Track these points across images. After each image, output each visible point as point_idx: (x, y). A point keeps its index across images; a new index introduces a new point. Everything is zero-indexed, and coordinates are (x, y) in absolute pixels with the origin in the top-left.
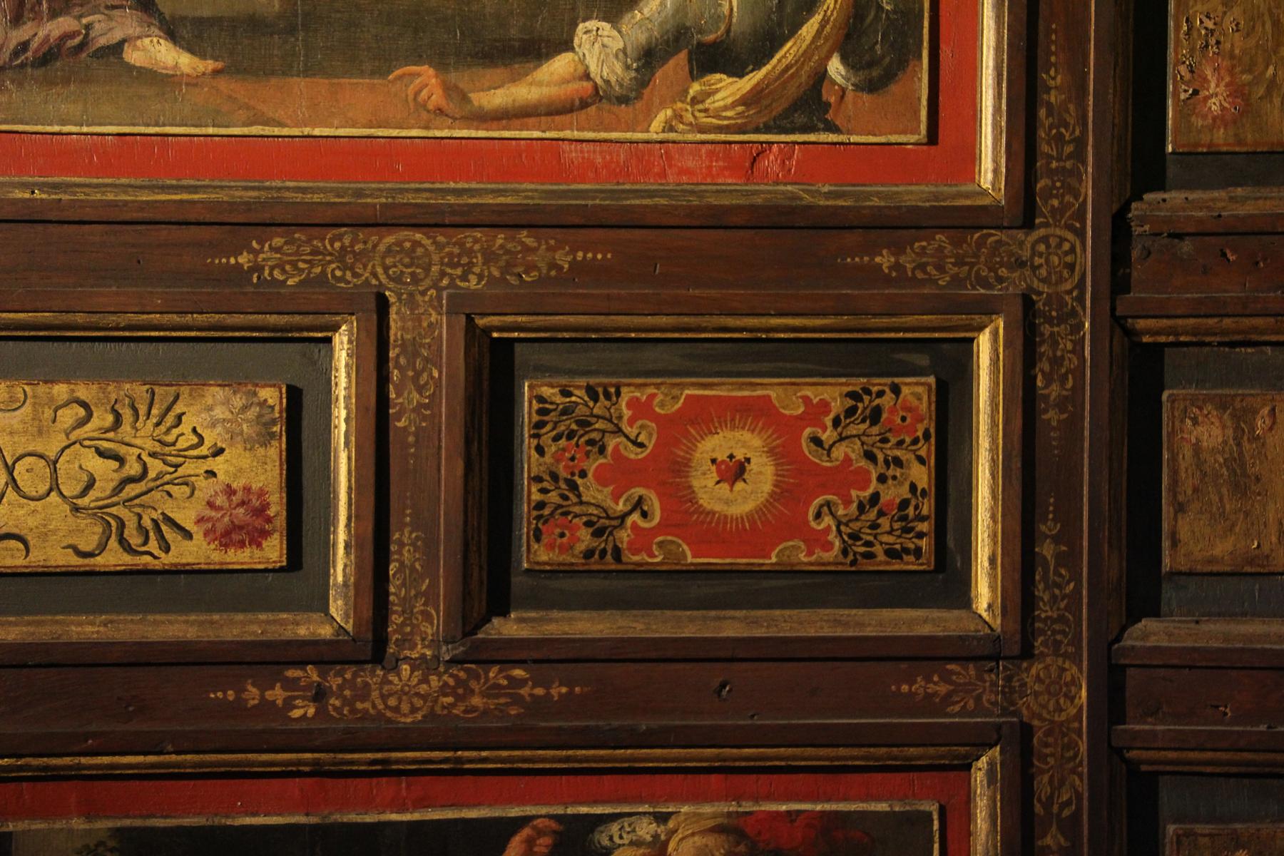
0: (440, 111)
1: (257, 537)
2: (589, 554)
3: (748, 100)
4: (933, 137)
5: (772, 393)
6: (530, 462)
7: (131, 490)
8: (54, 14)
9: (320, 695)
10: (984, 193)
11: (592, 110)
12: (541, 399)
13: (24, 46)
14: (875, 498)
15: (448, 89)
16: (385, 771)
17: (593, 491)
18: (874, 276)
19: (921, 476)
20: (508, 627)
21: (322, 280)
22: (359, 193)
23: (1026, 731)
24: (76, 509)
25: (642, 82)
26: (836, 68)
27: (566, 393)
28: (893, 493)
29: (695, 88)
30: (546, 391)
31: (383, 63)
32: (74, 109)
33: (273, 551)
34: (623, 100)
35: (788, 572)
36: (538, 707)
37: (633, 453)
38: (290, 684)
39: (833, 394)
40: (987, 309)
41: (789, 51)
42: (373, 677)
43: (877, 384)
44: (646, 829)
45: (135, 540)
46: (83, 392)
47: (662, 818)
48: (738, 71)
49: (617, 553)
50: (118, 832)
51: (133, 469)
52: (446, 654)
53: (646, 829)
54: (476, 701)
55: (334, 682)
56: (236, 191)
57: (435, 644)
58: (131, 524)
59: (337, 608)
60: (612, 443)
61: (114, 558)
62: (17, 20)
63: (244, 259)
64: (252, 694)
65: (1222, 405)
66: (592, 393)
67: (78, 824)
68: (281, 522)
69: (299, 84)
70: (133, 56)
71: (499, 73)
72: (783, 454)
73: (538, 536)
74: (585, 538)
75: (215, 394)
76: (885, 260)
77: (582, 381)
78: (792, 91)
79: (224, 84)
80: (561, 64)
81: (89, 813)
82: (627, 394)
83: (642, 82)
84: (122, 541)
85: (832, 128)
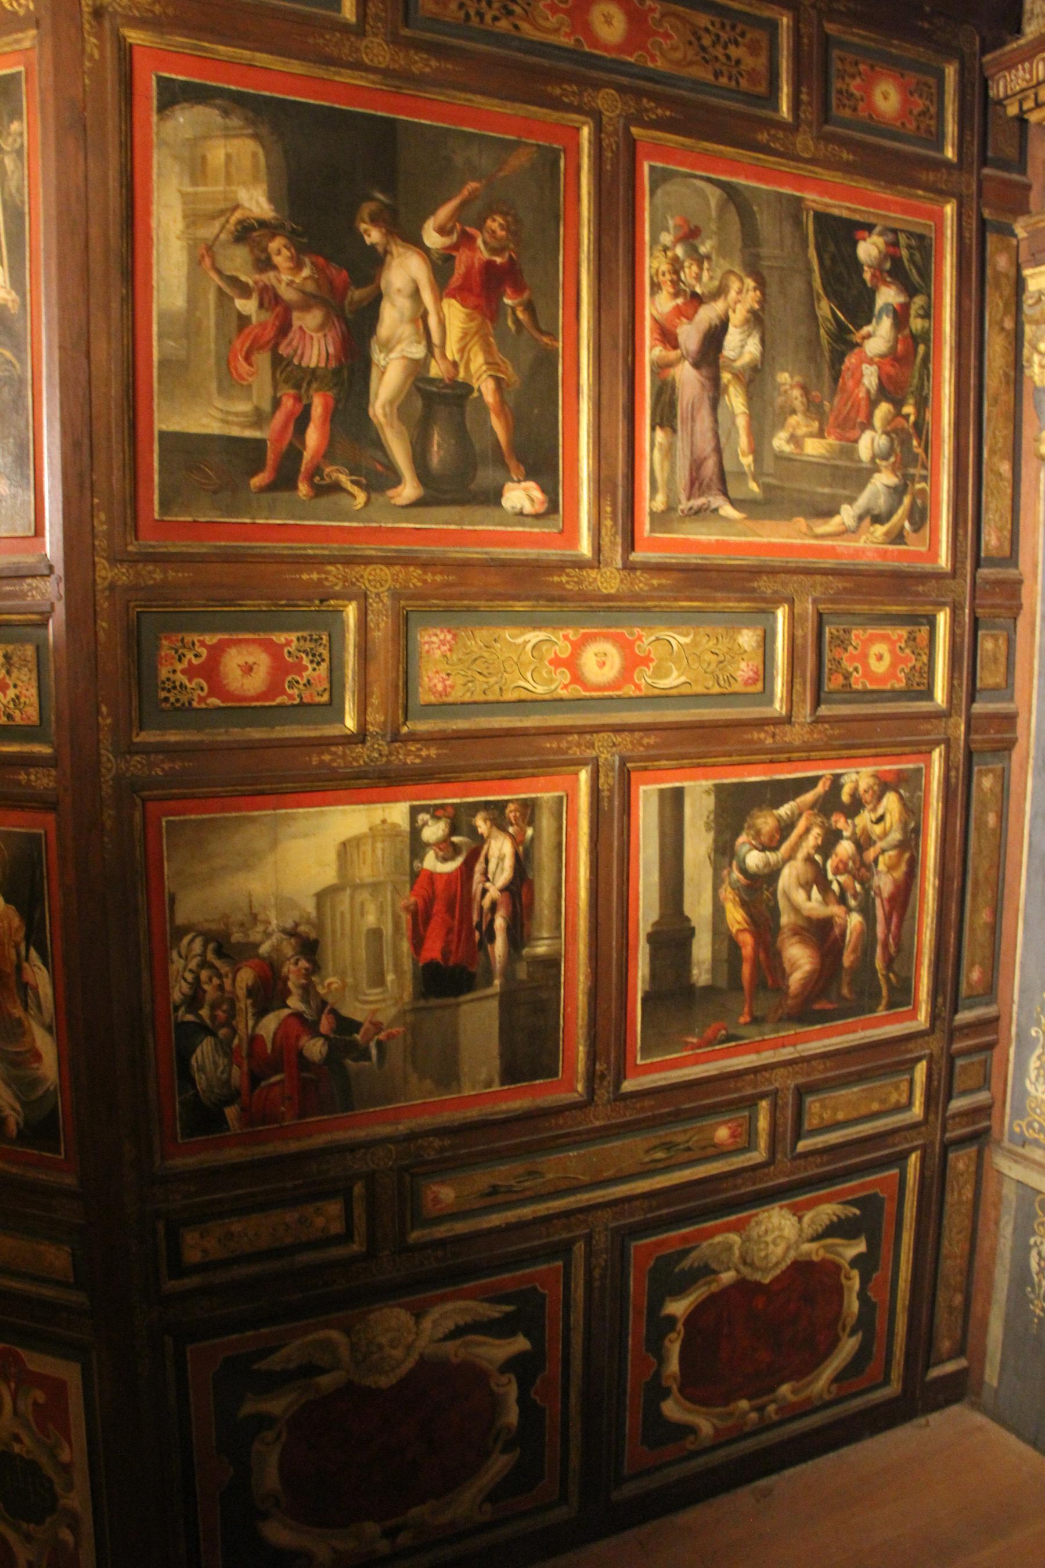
0: (805, 534)
1: (755, 681)
2: (843, 686)
3: (887, 534)
4: (930, 549)
5: (890, 632)
6: (827, 655)
7: (721, 665)
8: (700, 496)
9: (774, 735)
10: (942, 568)
11: (846, 536)
12: (831, 633)
13: (691, 508)
14: (914, 667)
15: (810, 528)
16: (789, 760)
17: (845, 663)
18: (917, 594)
19: (925, 659)
20: (824, 710)
21: (775, 592)
22: (787, 562)
23: (949, 739)
24: (706, 672)
25: (858, 527)
26: (907, 525)
27: (838, 631)
28: (918, 665)
29: (872, 529)
30: (834, 631)
31: (790, 516)
32: (704, 530)
33: (759, 686)
34: (854, 532)
35: (893, 691)
36: (831, 737)
37: (855, 652)
38: (766, 732)
39: (903, 632)
40: (944, 604)
41: (895, 519)
42: (787, 728)
43: (916, 628)
44: (854, 777)
45: (722, 683)
46: (708, 630)
47: (858, 773)
48: (882, 523)
49: (850, 685)
50: (716, 785)
51: (721, 658)
52: (809, 720)
53: (854, 777)
54: (815, 736)
55: (777, 731)
56: (750, 560)
57: (805, 717)
58: (721, 678)
59: (777, 705)
60: (850, 648)
61: (716, 690)
62: (689, 499)
63: (755, 585)
64: (755, 736)
65: (992, 636)
66: (844, 631)
67: (704, 783)
68: (762, 677)
69: (767, 523)
70: (722, 512)
71: (820, 521)
72: (892, 652)
73: (830, 679)
74: (841, 680)
75: (745, 632)
76: (920, 589)
77: (842, 627)
78: (896, 531)
79: (748, 523)
80: (836, 520)
81: (706, 777)
82: (854, 632)
83: (858, 527)
84: (718, 684)
85: (906, 544)
